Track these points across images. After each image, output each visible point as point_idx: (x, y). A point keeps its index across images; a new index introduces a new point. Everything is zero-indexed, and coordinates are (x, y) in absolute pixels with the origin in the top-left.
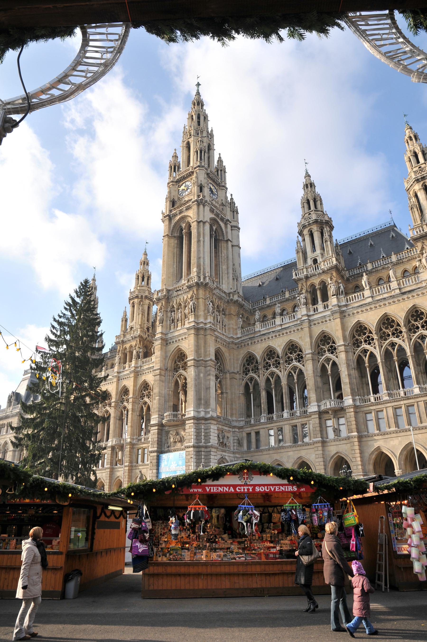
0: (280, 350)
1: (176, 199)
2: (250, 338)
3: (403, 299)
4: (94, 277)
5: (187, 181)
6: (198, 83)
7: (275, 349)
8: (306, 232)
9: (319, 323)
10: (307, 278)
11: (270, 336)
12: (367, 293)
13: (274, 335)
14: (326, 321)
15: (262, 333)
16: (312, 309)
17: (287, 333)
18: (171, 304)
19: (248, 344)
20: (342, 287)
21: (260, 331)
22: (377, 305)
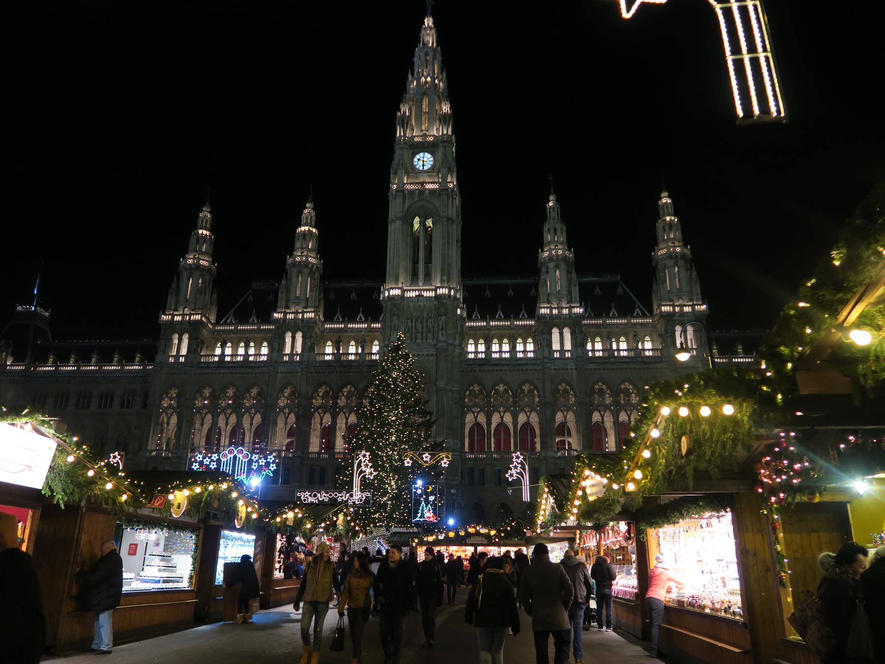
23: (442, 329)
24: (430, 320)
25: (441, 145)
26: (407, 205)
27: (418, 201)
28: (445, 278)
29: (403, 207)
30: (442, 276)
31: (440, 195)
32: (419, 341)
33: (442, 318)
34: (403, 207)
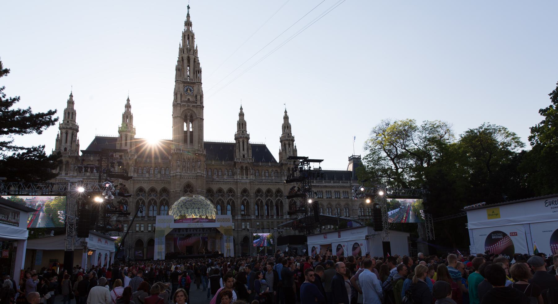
0: (225, 190)
1: (183, 94)
2: (211, 181)
3: (275, 184)
4: (71, 94)
5: (190, 86)
6: (188, 5)
7: (223, 189)
8: (241, 140)
9: (243, 184)
10: (241, 162)
11: (221, 183)
12: (263, 178)
13: (223, 183)
14: (246, 184)
15: (216, 180)
16: (241, 177)
17: (229, 184)
18: (183, 157)
19: (209, 183)
20: (254, 172)
21: (215, 179)
22: (266, 184)
23: (199, 167)
24: (193, 163)
25: (197, 84)
26: (182, 110)
27: (187, 109)
28: (199, 145)
29: (181, 112)
30: (198, 144)
31: (197, 107)
32: (189, 172)
33: (199, 163)
34: (181, 112)
